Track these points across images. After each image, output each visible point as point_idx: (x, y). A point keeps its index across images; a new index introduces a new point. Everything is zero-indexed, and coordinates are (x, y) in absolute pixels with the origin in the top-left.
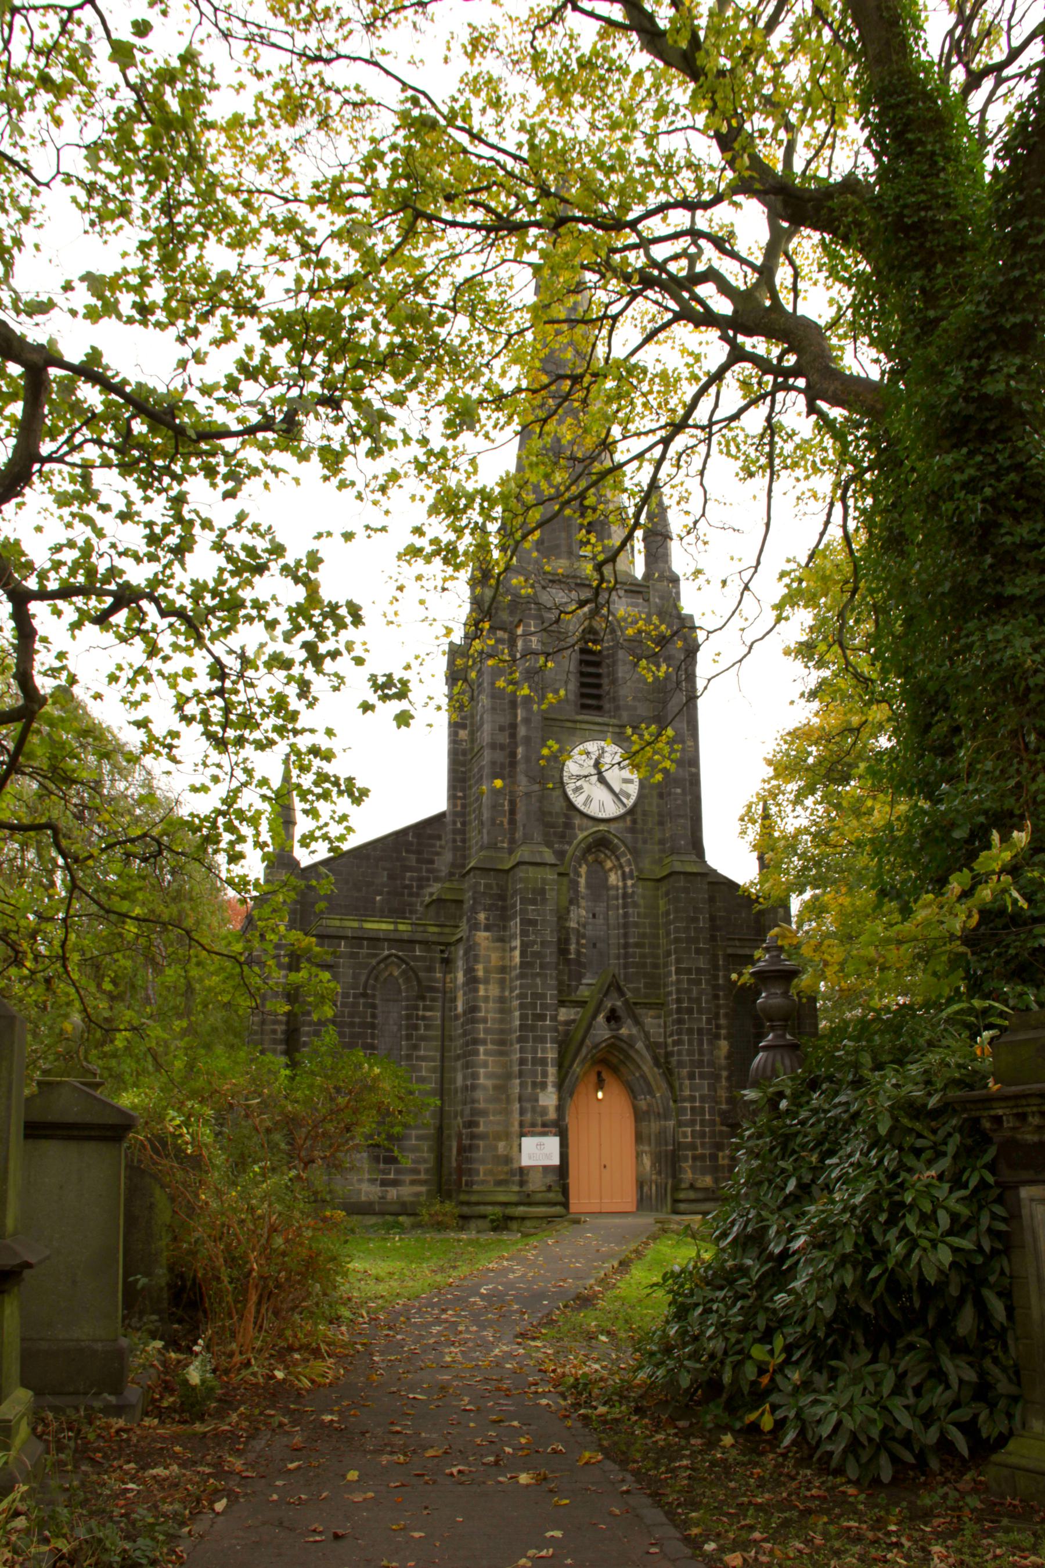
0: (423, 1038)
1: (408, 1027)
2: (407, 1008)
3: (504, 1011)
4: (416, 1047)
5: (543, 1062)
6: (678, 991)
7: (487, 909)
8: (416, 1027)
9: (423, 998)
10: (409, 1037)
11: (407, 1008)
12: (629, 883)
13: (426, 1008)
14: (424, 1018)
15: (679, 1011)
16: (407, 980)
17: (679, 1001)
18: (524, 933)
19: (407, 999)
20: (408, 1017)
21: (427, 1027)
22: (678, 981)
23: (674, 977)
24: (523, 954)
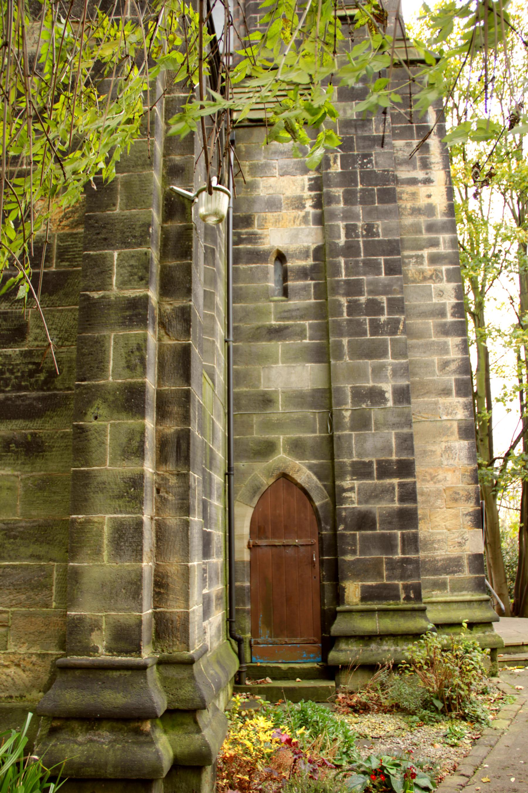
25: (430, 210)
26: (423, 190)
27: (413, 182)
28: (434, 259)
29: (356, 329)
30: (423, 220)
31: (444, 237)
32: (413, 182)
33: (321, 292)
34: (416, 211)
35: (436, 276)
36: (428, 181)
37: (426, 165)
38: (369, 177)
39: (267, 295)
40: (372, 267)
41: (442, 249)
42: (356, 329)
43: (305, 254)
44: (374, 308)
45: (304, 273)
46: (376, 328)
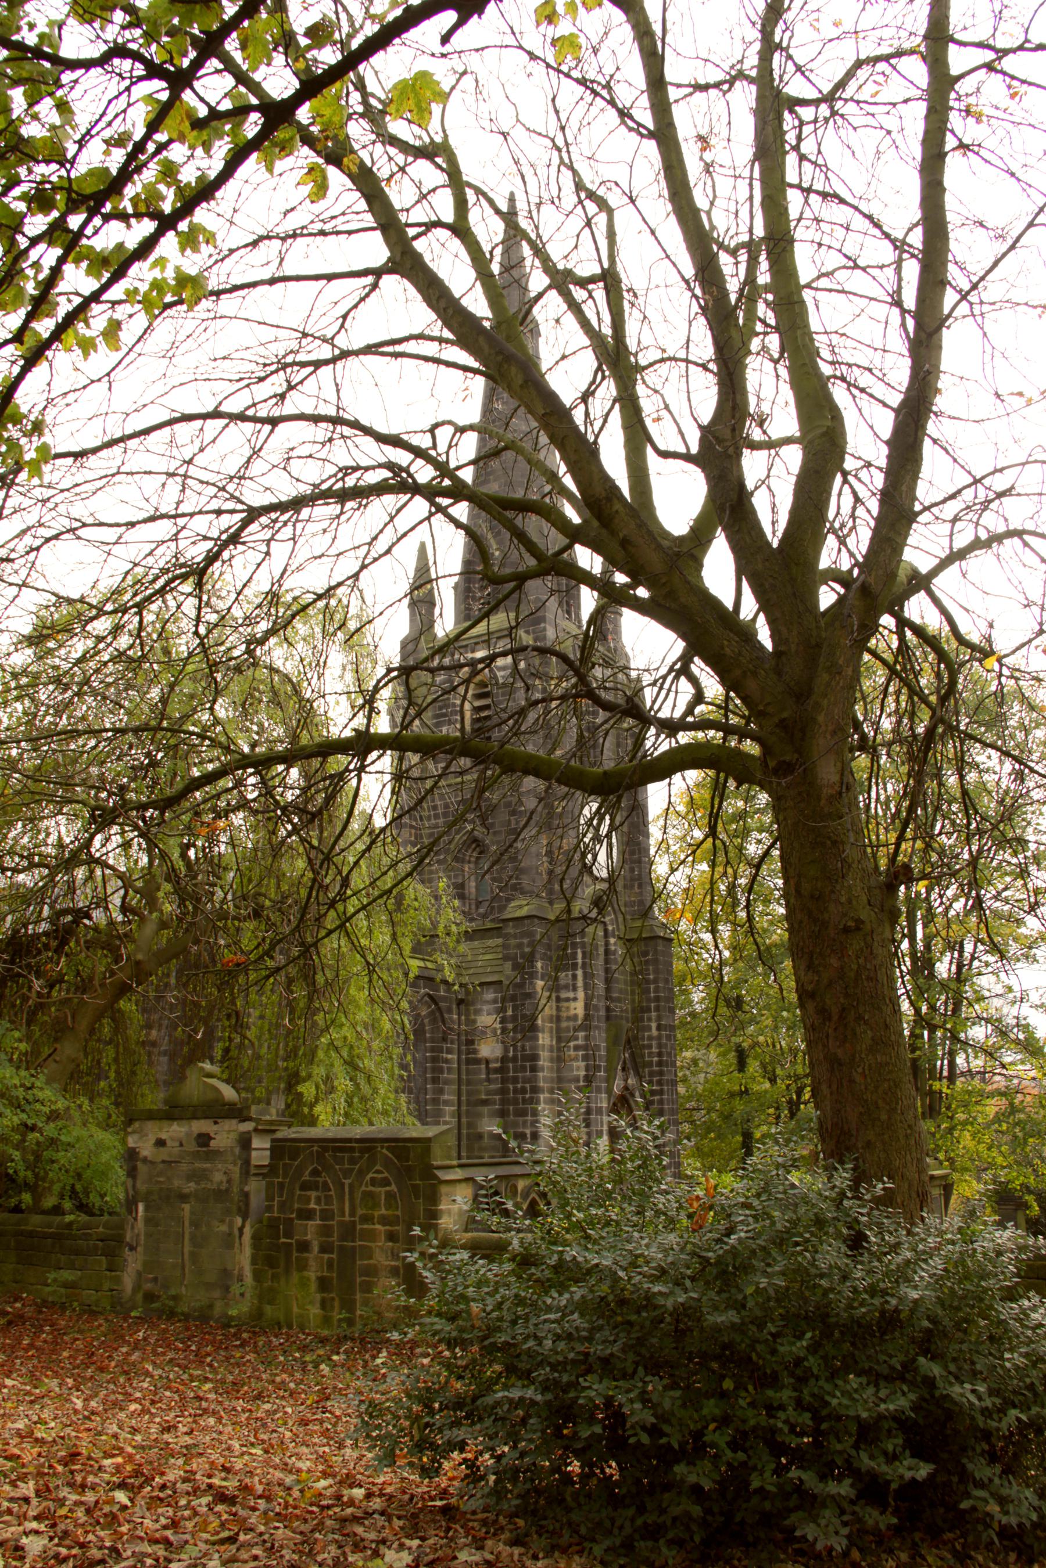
0: (447, 1082)
1: (434, 1070)
2: (433, 1049)
3: (559, 1059)
4: (441, 1091)
5: (599, 1111)
6: (660, 1046)
7: (545, 957)
8: (441, 1070)
9: (444, 1039)
10: (435, 1080)
11: (433, 1049)
12: (612, 940)
13: (449, 1052)
14: (447, 1061)
15: (660, 1064)
16: (434, 1021)
17: (660, 1054)
18: (586, 987)
20: (434, 1060)
22: (659, 1037)
24: (587, 1007)
25: (576, 1016)
26: (572, 1004)
27: (568, 1000)
28: (577, 1048)
29: (515, 1102)
31: (581, 1034)
32: (568, 1000)
33: (504, 1081)
34: (569, 1019)
35: (576, 1059)
36: (575, 999)
37: (575, 989)
38: (524, 1016)
40: (523, 1069)
41: (580, 1042)
42: (515, 1102)
43: (496, 1060)
44: (523, 1091)
45: (496, 1071)
46: (524, 1101)
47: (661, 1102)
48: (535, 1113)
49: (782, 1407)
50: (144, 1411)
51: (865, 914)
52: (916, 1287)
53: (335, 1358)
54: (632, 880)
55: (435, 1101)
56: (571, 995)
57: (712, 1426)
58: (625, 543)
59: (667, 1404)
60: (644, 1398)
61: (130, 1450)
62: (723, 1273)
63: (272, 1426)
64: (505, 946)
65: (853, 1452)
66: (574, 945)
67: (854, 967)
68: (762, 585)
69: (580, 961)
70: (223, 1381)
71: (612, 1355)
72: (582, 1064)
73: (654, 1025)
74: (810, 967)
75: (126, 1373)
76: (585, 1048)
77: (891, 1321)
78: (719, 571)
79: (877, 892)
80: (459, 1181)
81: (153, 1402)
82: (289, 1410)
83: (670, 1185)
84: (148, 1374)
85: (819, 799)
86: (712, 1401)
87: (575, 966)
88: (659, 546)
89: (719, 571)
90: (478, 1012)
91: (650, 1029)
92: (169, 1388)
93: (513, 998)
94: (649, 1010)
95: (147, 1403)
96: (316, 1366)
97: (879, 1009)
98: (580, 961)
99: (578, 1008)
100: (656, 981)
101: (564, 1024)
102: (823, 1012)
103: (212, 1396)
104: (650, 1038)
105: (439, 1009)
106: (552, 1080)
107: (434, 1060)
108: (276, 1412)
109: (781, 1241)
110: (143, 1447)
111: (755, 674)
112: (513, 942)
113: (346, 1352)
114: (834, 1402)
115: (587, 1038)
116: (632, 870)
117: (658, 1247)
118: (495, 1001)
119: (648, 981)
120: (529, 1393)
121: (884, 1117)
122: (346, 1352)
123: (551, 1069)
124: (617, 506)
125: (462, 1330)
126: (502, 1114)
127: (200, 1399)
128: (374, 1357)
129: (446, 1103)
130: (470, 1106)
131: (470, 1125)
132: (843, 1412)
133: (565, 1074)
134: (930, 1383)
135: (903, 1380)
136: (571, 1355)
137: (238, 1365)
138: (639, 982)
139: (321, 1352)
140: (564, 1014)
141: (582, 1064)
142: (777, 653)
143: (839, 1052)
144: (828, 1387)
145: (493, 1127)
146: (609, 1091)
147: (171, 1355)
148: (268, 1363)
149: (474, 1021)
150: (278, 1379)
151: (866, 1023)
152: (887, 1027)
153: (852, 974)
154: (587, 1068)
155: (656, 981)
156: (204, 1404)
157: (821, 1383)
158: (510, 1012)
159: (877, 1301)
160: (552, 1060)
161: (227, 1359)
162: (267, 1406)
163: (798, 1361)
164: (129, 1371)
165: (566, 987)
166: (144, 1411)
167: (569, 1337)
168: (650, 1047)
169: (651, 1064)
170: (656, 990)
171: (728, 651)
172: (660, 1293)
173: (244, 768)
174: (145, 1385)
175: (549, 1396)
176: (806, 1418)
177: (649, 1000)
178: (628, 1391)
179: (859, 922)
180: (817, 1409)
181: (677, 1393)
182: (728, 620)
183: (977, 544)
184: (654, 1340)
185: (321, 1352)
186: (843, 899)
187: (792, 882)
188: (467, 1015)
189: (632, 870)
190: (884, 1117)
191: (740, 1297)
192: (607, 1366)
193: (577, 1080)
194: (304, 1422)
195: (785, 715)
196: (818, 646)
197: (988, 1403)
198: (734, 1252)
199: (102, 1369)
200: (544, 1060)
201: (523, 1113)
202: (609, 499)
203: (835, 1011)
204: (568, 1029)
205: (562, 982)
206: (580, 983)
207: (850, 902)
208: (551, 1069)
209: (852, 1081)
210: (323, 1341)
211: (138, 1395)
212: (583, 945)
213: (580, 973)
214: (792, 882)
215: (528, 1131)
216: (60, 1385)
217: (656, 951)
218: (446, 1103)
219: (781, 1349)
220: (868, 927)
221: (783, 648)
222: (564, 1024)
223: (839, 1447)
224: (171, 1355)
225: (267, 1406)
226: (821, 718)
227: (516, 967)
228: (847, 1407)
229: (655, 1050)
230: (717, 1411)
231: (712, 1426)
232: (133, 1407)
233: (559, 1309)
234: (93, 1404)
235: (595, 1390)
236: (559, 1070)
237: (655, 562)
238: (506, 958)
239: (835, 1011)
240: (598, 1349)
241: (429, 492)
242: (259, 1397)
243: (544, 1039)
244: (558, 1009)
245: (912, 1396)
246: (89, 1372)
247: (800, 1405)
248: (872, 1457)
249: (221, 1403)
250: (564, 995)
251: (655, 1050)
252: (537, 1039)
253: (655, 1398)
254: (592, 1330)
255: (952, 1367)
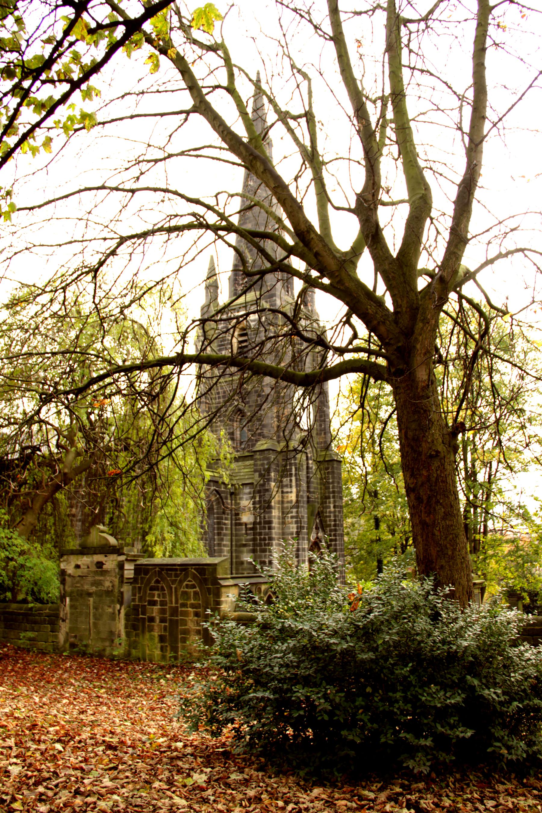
0: (225, 535)
1: (218, 529)
2: (218, 518)
4: (222, 540)
5: (304, 550)
6: (335, 516)
7: (276, 471)
8: (222, 529)
9: (224, 513)
10: (219, 534)
11: (218, 518)
12: (310, 462)
14: (225, 524)
15: (335, 525)
16: (218, 503)
17: (335, 521)
18: (297, 486)
19: (218, 513)
20: (219, 523)
21: (226, 529)
22: (335, 512)
23: (332, 509)
24: (297, 496)
25: (291, 502)
26: (290, 495)
27: (287, 492)
28: (292, 517)
29: (260, 545)
30: (289, 505)
31: (294, 510)
32: (287, 492)
33: (254, 534)
34: (288, 502)
35: (292, 523)
36: (291, 492)
37: (291, 487)
38: (265, 501)
39: (242, 535)
40: (264, 528)
41: (294, 514)
42: (260, 545)
43: (251, 524)
44: (265, 539)
45: (251, 529)
46: (265, 545)
47: (335, 545)
48: (270, 551)
49: (397, 701)
50: (70, 703)
51: (441, 448)
52: (466, 640)
53: (168, 676)
54: (321, 430)
55: (219, 545)
56: (289, 490)
57: (360, 711)
58: (317, 255)
59: (337, 700)
60: (326, 697)
61: (63, 723)
62: (366, 633)
63: (136, 711)
64: (255, 465)
65: (433, 724)
66: (291, 464)
67: (435, 475)
68: (388, 277)
69: (293, 472)
70: (110, 688)
71: (309, 675)
72: (295, 526)
73: (332, 505)
74: (412, 475)
75: (61, 684)
76: (297, 517)
77: (453, 657)
78: (366, 271)
79: (447, 436)
80: (232, 586)
81: (75, 699)
82: (144, 703)
83: (340, 587)
84: (72, 684)
85: (417, 388)
86: (361, 698)
87: (291, 475)
88: (334, 257)
89: (366, 271)
90: (241, 499)
91: (330, 507)
92: (83, 692)
93: (259, 492)
94: (329, 498)
95: (72, 699)
96: (158, 680)
97: (448, 497)
98: (293, 472)
99: (293, 497)
100: (333, 483)
101: (285, 505)
102: (419, 499)
103: (105, 696)
104: (330, 512)
105: (221, 497)
106: (279, 534)
107: (219, 523)
108: (137, 703)
109: (396, 616)
110: (69, 722)
111: (384, 323)
112: (259, 463)
113: (173, 673)
114: (424, 698)
115: (297, 512)
116: (321, 425)
117: (333, 619)
118: (250, 493)
119: (329, 483)
120: (267, 694)
121: (450, 553)
122: (173, 673)
123: (279, 528)
124: (312, 235)
125: (232, 662)
126: (254, 551)
127: (98, 697)
128: (188, 676)
129: (225, 546)
130: (237, 547)
131: (237, 557)
132: (428, 704)
133: (286, 531)
134: (472, 688)
135: (460, 688)
136: (288, 675)
137: (118, 680)
138: (324, 484)
139: (161, 673)
140: (285, 500)
141: (295, 526)
142: (396, 312)
143: (427, 519)
144: (420, 691)
145: (248, 558)
146: (309, 539)
147: (84, 675)
148: (134, 679)
149: (239, 504)
150: (139, 687)
151: (441, 504)
152: (452, 506)
153: (434, 479)
154: (297, 528)
155: (333, 483)
156: (101, 700)
157: (417, 689)
158: (257, 499)
159: (445, 647)
160: (279, 523)
161: (113, 677)
162: (133, 701)
163: (405, 677)
164: (62, 683)
165: (286, 486)
166: (70, 703)
167: (287, 666)
168: (330, 516)
169: (330, 526)
170: (333, 487)
171: (370, 311)
172: (334, 643)
173: (119, 372)
174: (71, 690)
175: (277, 696)
176: (409, 707)
177: (329, 493)
178: (318, 693)
179: (438, 452)
180: (415, 701)
181: (343, 694)
182: (370, 295)
183: (500, 256)
184: (331, 667)
185: (161, 673)
186: (429, 440)
187: (403, 431)
188: (236, 500)
189: (321, 425)
190: (450, 553)
191: (375, 645)
192: (306, 681)
193: (292, 534)
194: (152, 709)
195: (400, 344)
196: (417, 309)
197: (502, 699)
198: (372, 622)
199: (49, 682)
200: (275, 524)
201: (264, 551)
202: (308, 232)
203: (425, 498)
204: (287, 508)
205: (284, 483)
206: (294, 484)
207: (433, 442)
208: (279, 528)
209: (433, 534)
210: (162, 668)
211: (67, 695)
212: (295, 464)
213: (293, 478)
214: (403, 431)
215: (267, 560)
216: (27, 690)
217: (333, 467)
218: (225, 546)
219: (397, 672)
220: (442, 455)
221: (399, 310)
222: (285, 505)
223: (425, 721)
224: (84, 675)
225: (133, 701)
226: (418, 346)
227: (261, 475)
228: (430, 701)
229: (332, 518)
230: (363, 703)
231: (360, 711)
232: (65, 701)
233: (282, 651)
234: (44, 699)
235: (300, 692)
236: (283, 529)
237: (333, 265)
238: (255, 471)
239: (425, 498)
240: (302, 672)
241: (215, 229)
242: (129, 696)
243: (275, 513)
244: (283, 497)
245: (463, 696)
246: (42, 684)
247: (406, 700)
248: (442, 727)
249: (109, 699)
250: (285, 490)
251: (332, 518)
252: (271, 512)
253: (331, 697)
254: (299, 662)
255: (484, 681)
